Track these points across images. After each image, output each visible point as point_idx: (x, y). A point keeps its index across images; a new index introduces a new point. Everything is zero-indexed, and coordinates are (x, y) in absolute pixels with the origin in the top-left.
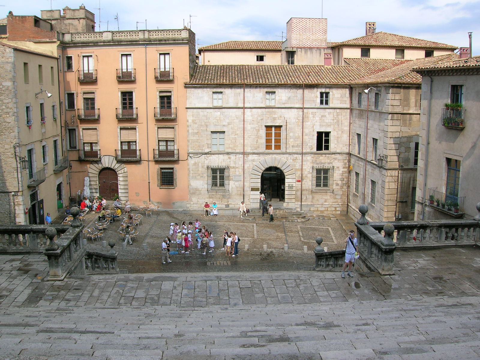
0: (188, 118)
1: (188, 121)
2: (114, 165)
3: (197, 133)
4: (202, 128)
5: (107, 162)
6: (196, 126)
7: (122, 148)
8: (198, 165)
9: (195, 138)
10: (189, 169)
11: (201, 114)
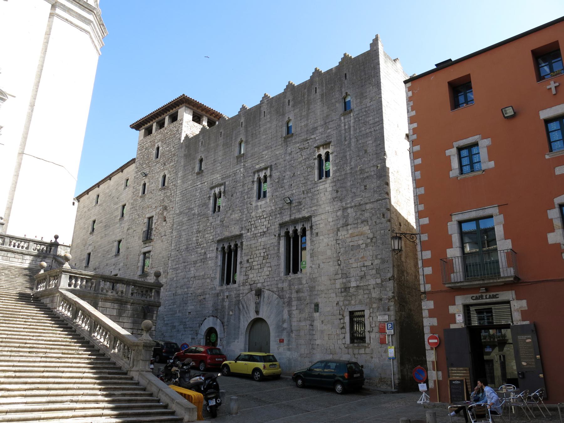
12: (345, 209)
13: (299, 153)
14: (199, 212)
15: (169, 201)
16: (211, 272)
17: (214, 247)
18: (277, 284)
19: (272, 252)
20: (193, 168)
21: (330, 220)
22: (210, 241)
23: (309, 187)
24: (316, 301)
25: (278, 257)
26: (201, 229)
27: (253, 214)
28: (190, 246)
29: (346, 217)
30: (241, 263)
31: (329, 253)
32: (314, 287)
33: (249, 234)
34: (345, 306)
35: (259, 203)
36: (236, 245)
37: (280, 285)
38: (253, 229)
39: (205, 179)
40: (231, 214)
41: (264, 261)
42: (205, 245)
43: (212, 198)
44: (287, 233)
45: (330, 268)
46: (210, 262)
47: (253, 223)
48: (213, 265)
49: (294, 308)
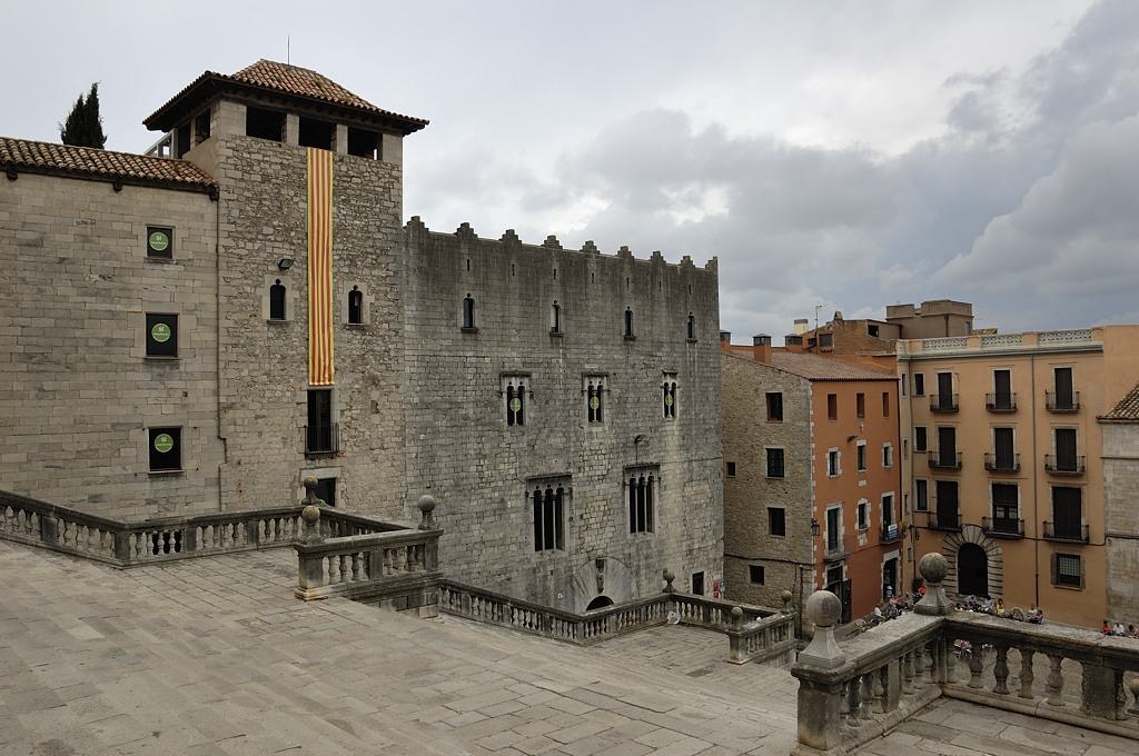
0: (1105, 475)
1: (1105, 480)
2: (981, 541)
3: (1121, 501)
4: (1131, 493)
5: (971, 535)
6: (1120, 488)
7: (995, 515)
8: (1125, 556)
9: (1118, 510)
10: (1107, 561)
11: (1132, 468)
12: (690, 461)
13: (644, 371)
14: (479, 416)
15: (384, 367)
16: (518, 533)
17: (521, 489)
18: (623, 550)
19: (615, 506)
20: (452, 315)
21: (678, 472)
22: (509, 477)
23: (657, 424)
24: (664, 567)
25: (624, 513)
26: (487, 452)
27: (586, 444)
28: (465, 482)
29: (691, 471)
30: (571, 519)
31: (677, 511)
32: (662, 552)
33: (581, 475)
34: (689, 569)
35: (594, 430)
36: (560, 491)
37: (626, 551)
38: (587, 469)
39: (484, 349)
40: (548, 436)
41: (605, 518)
42: (500, 484)
43: (505, 395)
44: (632, 480)
45: (677, 529)
46: (513, 516)
47: (586, 458)
48: (520, 521)
49: (643, 578)
